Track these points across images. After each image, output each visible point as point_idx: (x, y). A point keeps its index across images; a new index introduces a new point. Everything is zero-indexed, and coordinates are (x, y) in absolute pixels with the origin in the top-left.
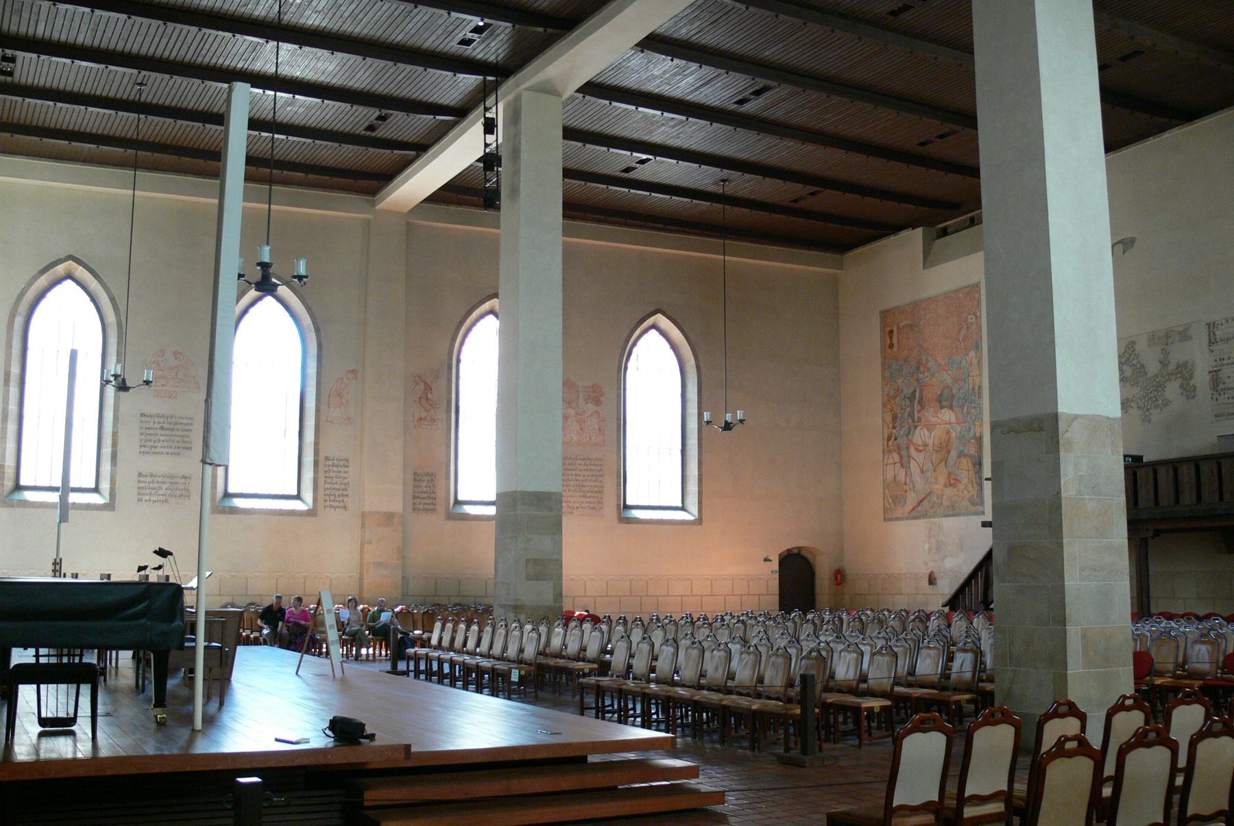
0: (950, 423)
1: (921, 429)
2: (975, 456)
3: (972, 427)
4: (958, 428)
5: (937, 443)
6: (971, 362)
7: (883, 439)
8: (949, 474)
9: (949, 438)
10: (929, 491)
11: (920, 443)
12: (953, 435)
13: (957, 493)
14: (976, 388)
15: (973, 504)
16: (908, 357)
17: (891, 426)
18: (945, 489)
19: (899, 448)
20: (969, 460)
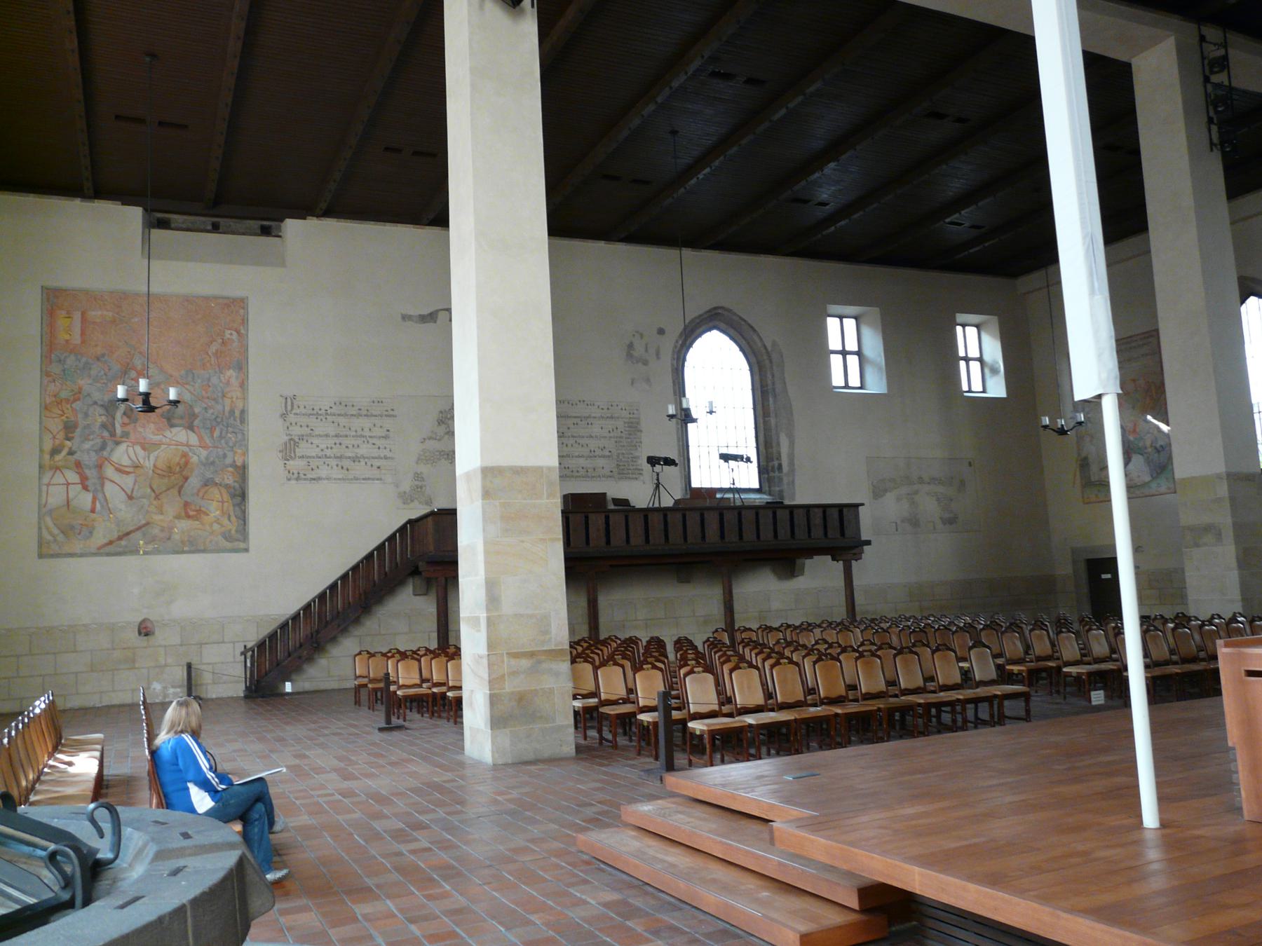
0: (187, 445)
1: (128, 446)
2: (234, 488)
3: (230, 454)
4: (204, 453)
5: (160, 465)
6: (228, 381)
7: (41, 450)
8: (186, 504)
9: (187, 463)
10: (143, 522)
11: (125, 461)
12: (195, 459)
13: (200, 526)
14: (237, 413)
15: (227, 537)
16: (103, 355)
17: (61, 436)
18: (176, 521)
19: (78, 465)
20: (223, 491)
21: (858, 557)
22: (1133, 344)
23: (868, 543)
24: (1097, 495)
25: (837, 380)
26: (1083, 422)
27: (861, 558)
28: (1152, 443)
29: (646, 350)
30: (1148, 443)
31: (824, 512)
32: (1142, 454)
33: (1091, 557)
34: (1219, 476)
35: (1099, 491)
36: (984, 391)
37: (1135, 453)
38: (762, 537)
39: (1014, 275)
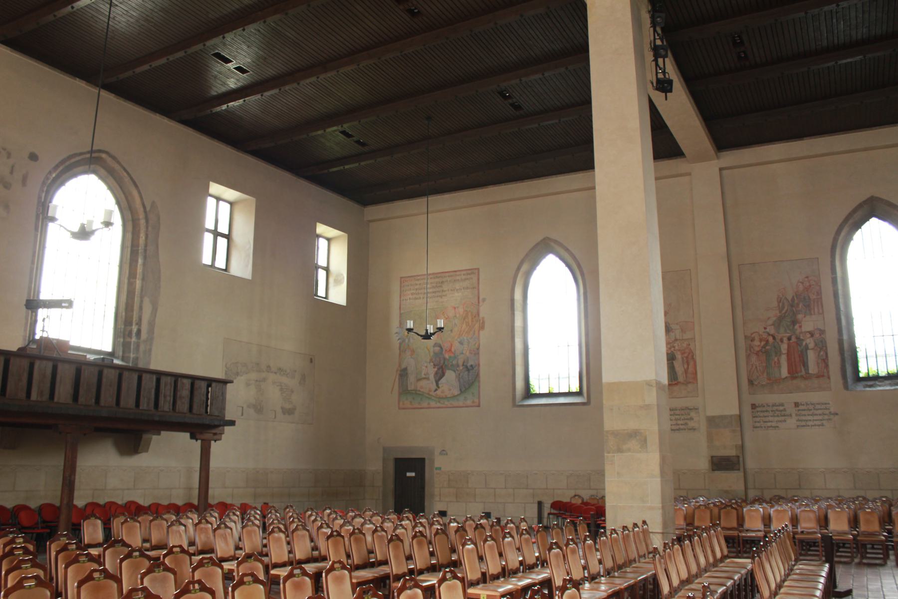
21: (217, 437)
22: (458, 278)
23: (232, 423)
24: (411, 402)
25: (206, 259)
26: (443, 328)
27: (220, 439)
28: (464, 362)
29: (11, 173)
30: (460, 363)
31: (192, 385)
32: (454, 371)
33: (400, 456)
34: (648, 384)
35: (414, 399)
36: (326, 298)
37: (449, 369)
38: (122, 404)
39: (365, 202)
